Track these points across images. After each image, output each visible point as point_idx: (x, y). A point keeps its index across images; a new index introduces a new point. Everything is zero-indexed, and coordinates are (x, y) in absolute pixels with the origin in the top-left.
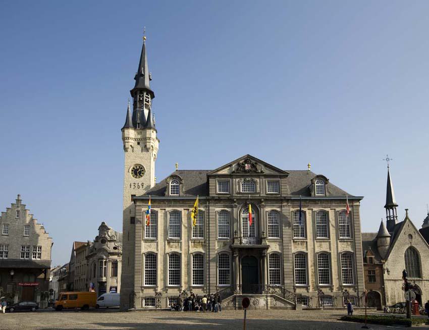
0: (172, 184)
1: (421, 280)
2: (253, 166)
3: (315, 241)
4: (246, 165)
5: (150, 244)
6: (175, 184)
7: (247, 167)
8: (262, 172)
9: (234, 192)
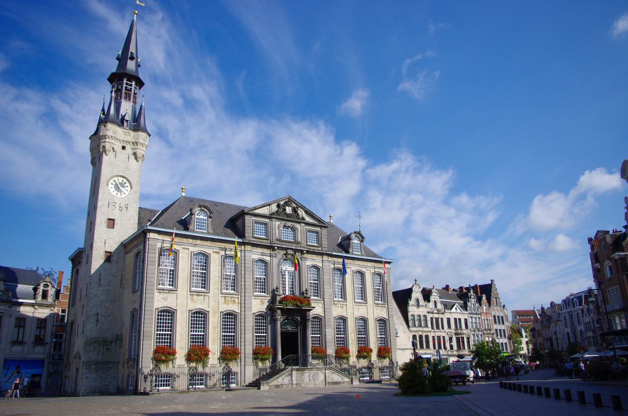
2: (295, 210)
3: (354, 304)
4: (287, 208)
5: (165, 295)
7: (289, 210)
8: (303, 219)
9: (274, 239)
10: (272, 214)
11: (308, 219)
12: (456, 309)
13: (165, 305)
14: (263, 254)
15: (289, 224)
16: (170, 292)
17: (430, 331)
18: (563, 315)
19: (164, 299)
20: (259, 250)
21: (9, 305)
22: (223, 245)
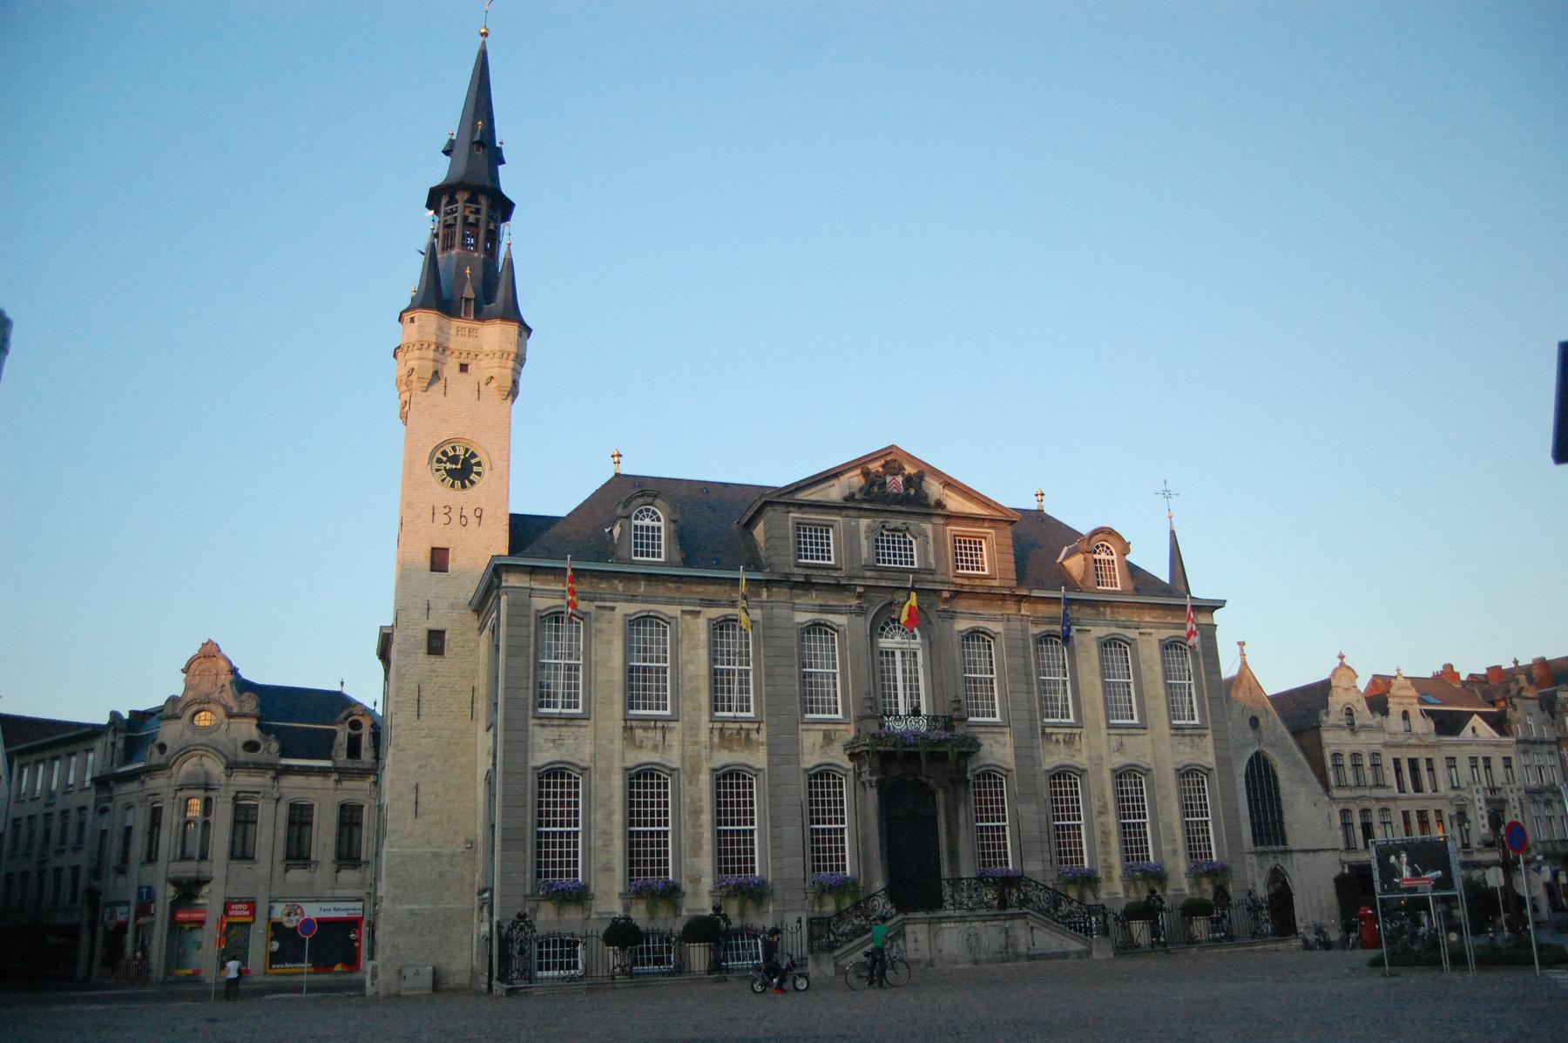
0: (639, 523)
1: (1292, 851)
2: (909, 480)
4: (889, 479)
6: (647, 522)
8: (939, 504)
10: (846, 499)
12: (1474, 730)
13: (558, 758)
14: (825, 609)
16: (570, 723)
17: (1394, 799)
19: (554, 741)
20: (814, 598)
21: (271, 773)
22: (711, 591)
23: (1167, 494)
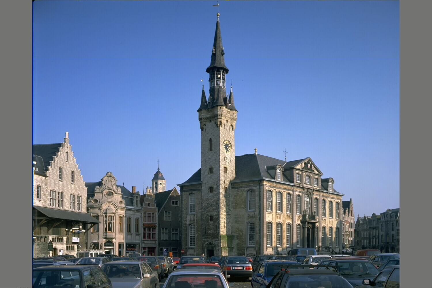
2: (311, 166)
11: (316, 172)
15: (309, 174)
18: (381, 223)
23: (285, 152)
